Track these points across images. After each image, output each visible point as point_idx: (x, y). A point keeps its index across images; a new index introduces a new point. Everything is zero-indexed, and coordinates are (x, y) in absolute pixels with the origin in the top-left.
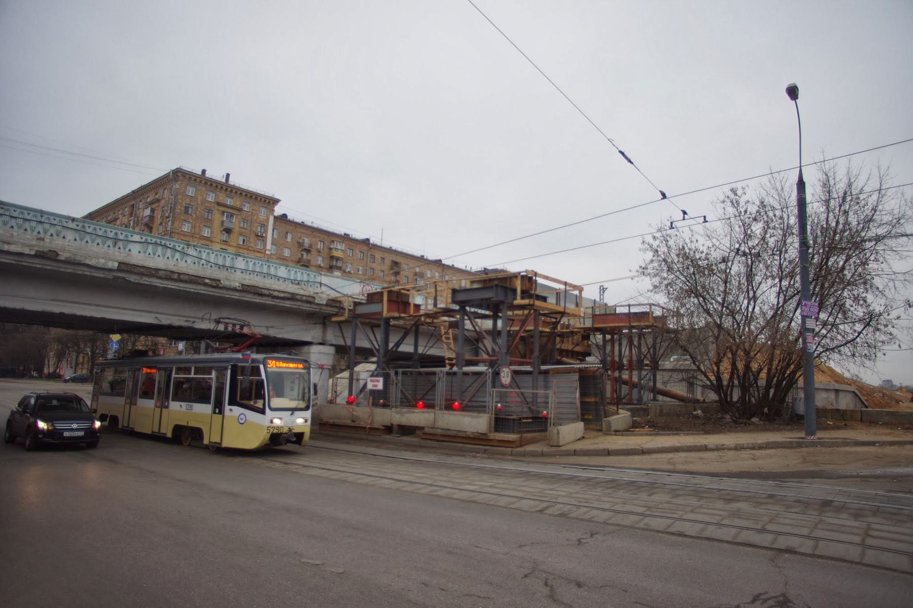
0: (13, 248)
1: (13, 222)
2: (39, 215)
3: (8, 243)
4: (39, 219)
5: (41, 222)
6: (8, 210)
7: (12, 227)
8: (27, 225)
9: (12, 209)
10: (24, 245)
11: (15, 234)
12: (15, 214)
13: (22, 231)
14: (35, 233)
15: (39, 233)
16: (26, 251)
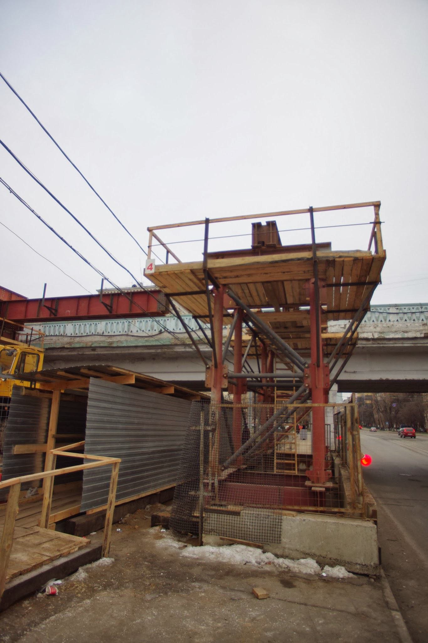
0: (410, 335)
1: (406, 317)
2: (419, 307)
3: (406, 332)
4: (421, 311)
5: (422, 312)
6: (401, 309)
7: (406, 320)
8: (414, 316)
9: (403, 308)
10: (416, 331)
11: (409, 325)
12: (405, 311)
13: (412, 321)
14: (420, 321)
15: (423, 320)
16: (418, 335)
